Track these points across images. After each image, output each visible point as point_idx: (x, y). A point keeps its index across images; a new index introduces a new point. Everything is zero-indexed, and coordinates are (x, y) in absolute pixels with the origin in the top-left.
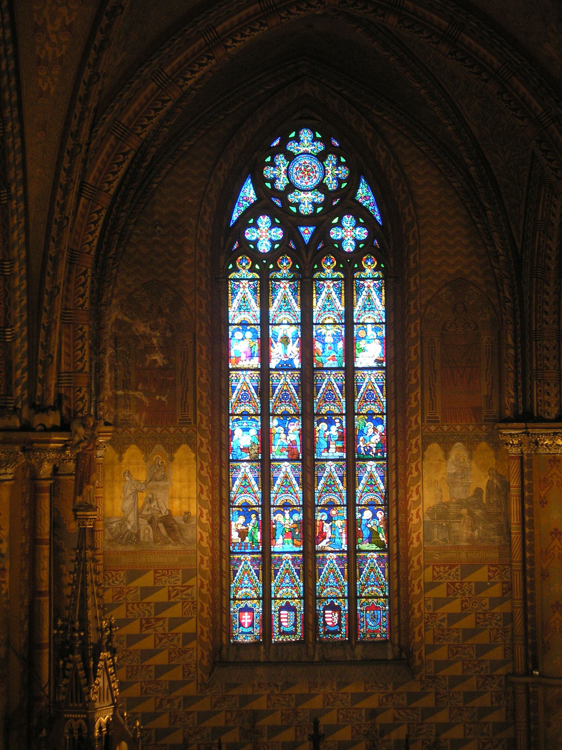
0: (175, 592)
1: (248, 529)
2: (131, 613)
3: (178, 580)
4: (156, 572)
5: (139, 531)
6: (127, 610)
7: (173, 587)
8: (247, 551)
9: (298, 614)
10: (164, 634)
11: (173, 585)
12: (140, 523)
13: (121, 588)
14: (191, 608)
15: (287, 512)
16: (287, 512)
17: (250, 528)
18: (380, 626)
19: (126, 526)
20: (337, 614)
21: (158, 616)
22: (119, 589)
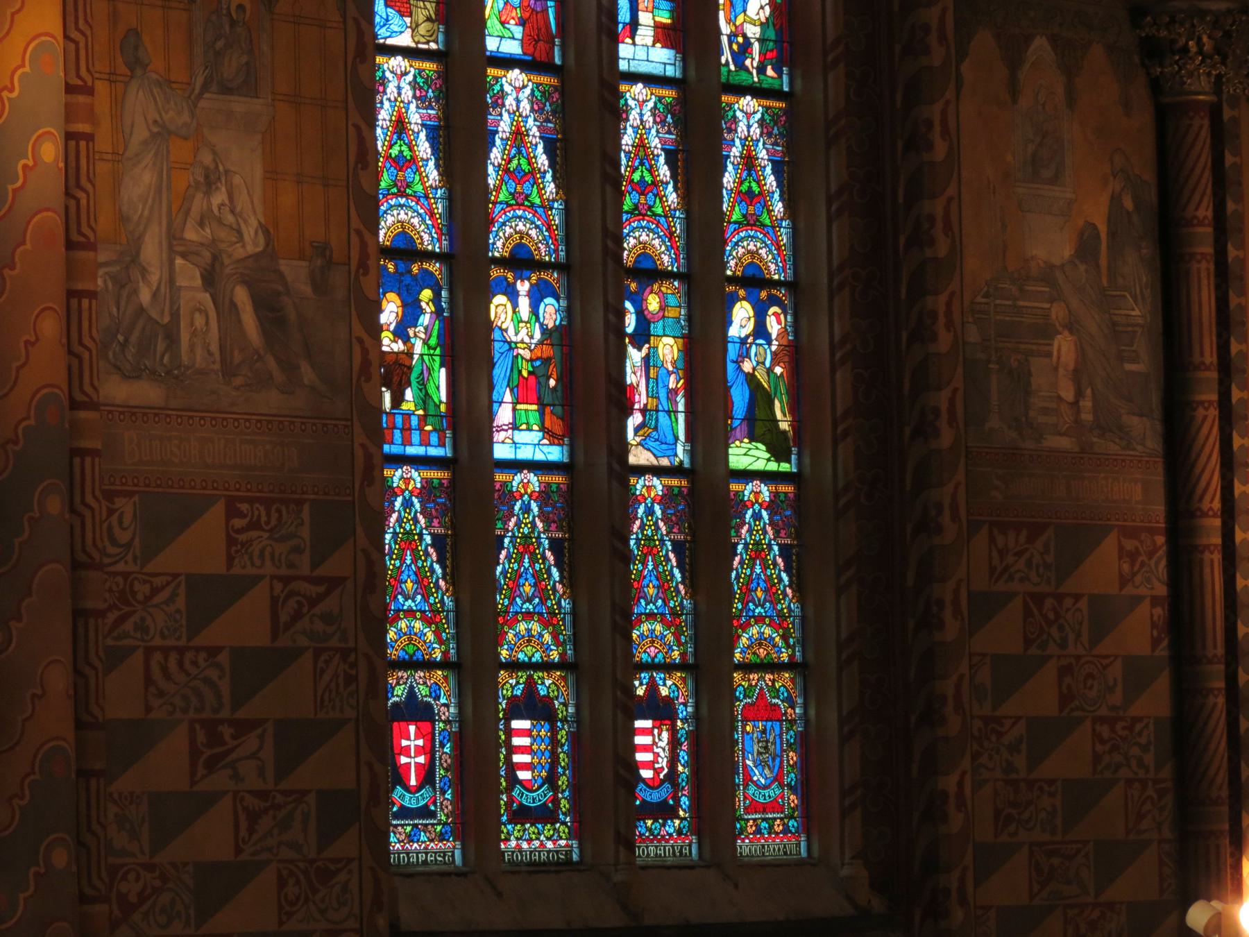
0: (292, 604)
1: (410, 354)
2: (161, 694)
3: (297, 550)
4: (232, 511)
5: (175, 316)
6: (149, 680)
7: (286, 580)
8: (411, 450)
9: (562, 735)
10: (262, 795)
11: (283, 571)
12: (181, 282)
13: (126, 575)
14: (341, 680)
15: (523, 287)
16: (523, 287)
17: (419, 348)
18: (782, 785)
19: (135, 292)
20: (665, 735)
21: (241, 714)
22: (120, 579)
